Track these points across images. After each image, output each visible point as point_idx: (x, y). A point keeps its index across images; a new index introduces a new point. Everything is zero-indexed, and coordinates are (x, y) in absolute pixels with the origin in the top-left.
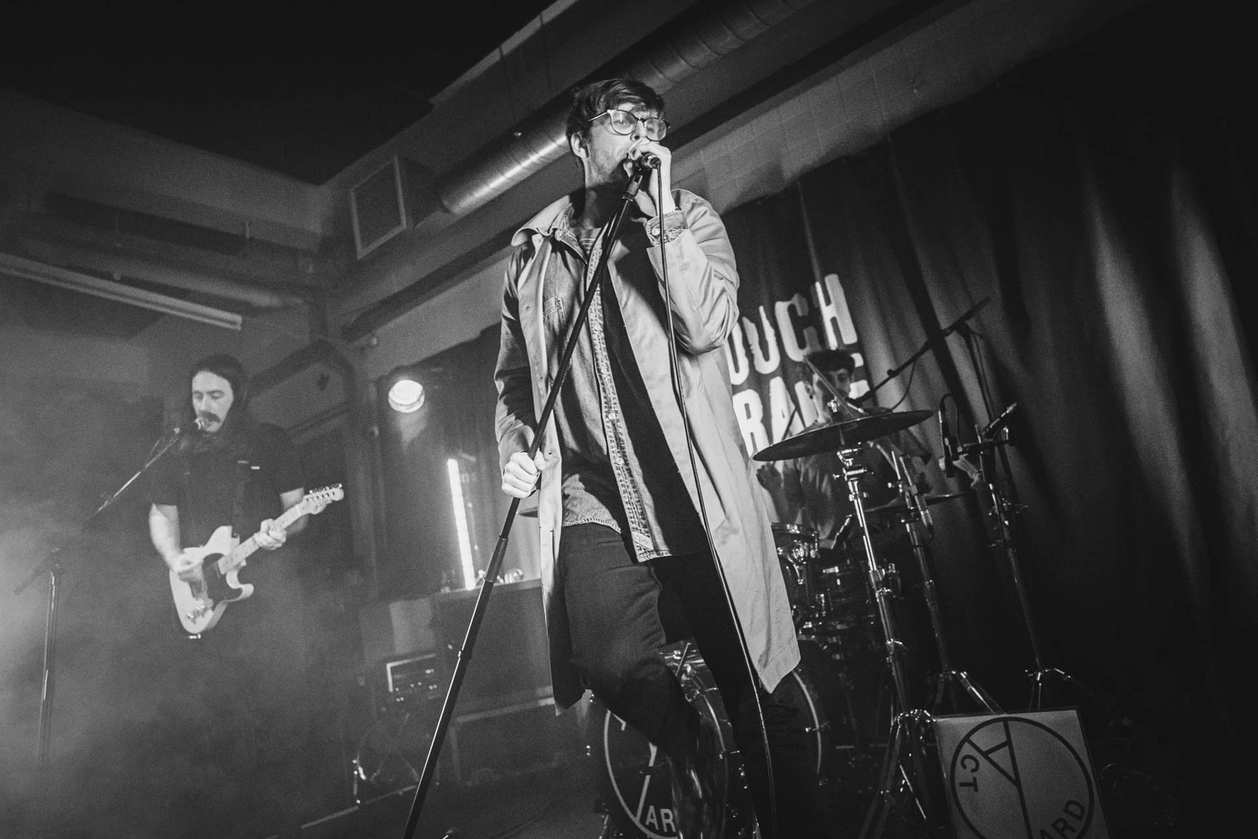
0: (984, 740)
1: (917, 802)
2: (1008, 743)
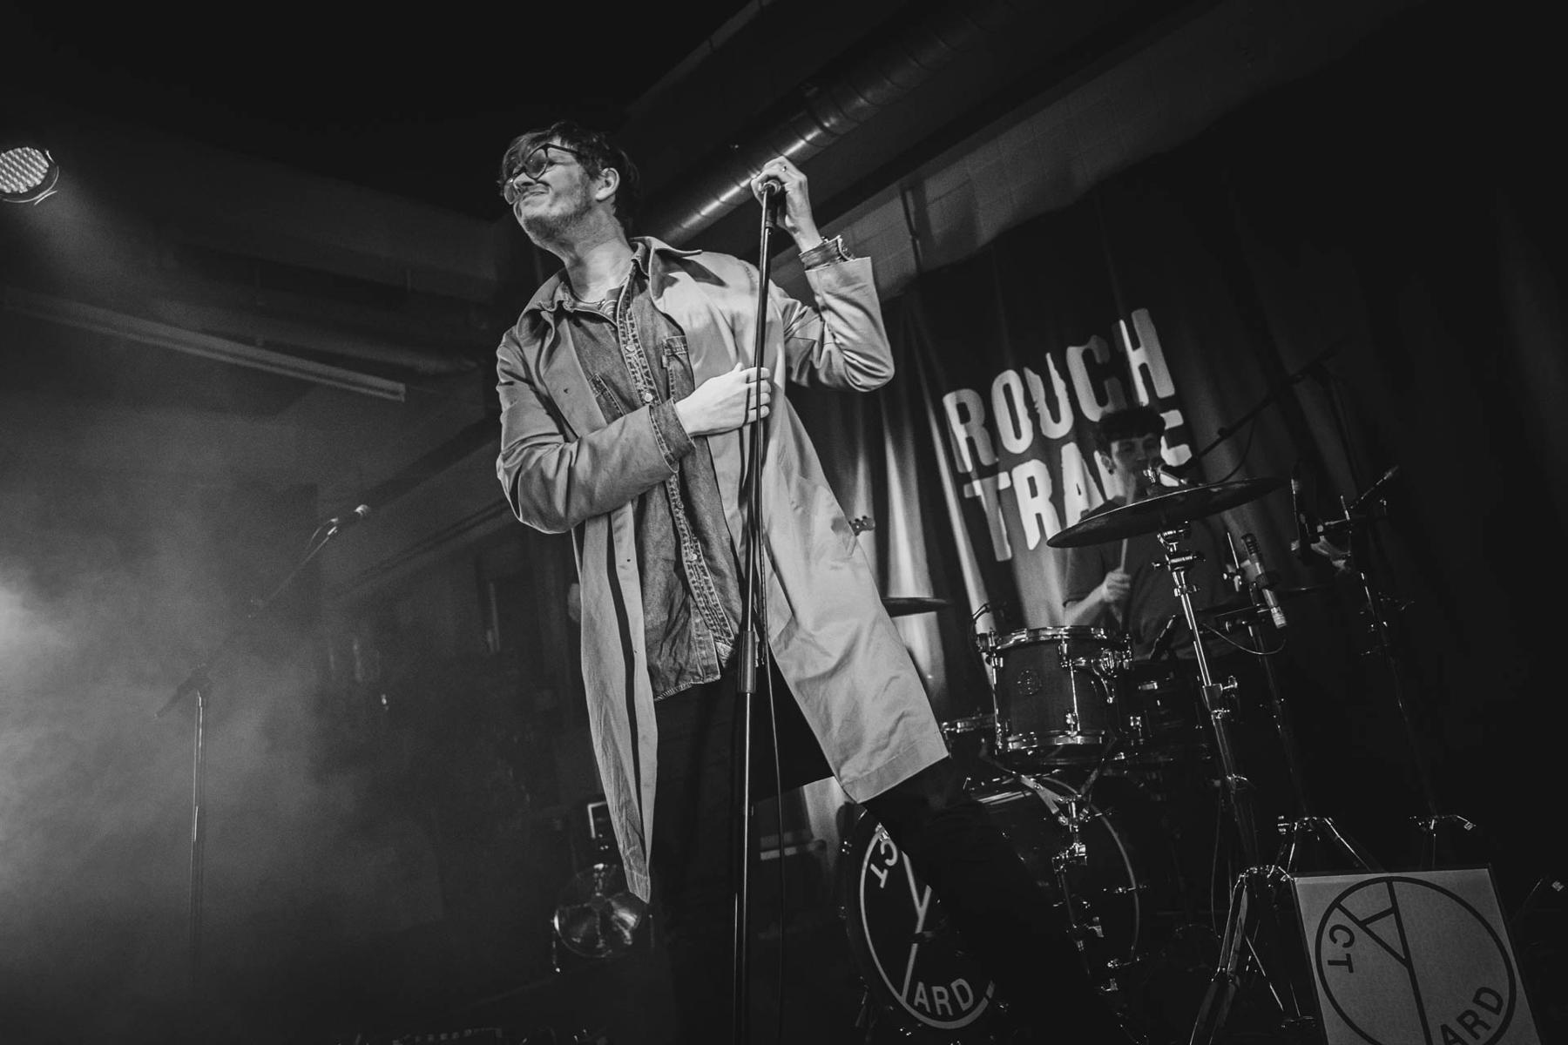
0: (1360, 905)
2: (1394, 910)
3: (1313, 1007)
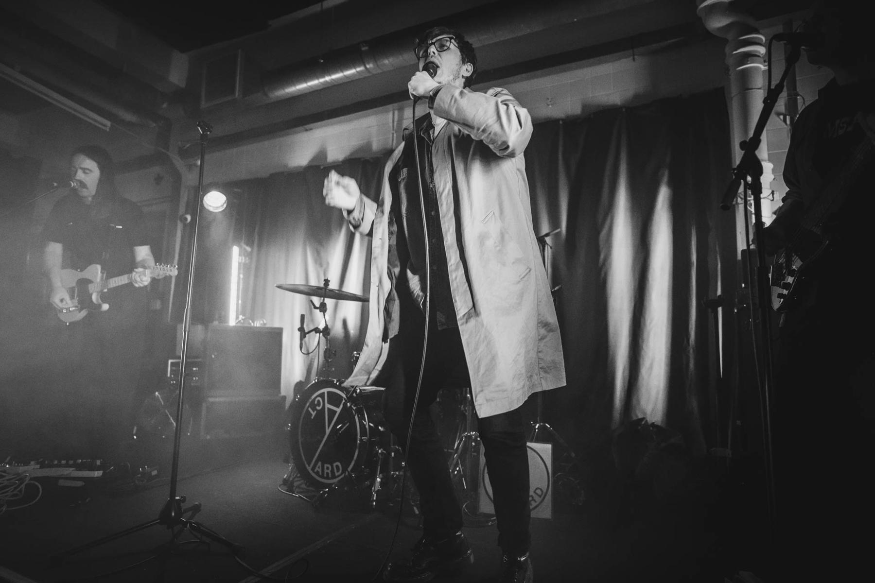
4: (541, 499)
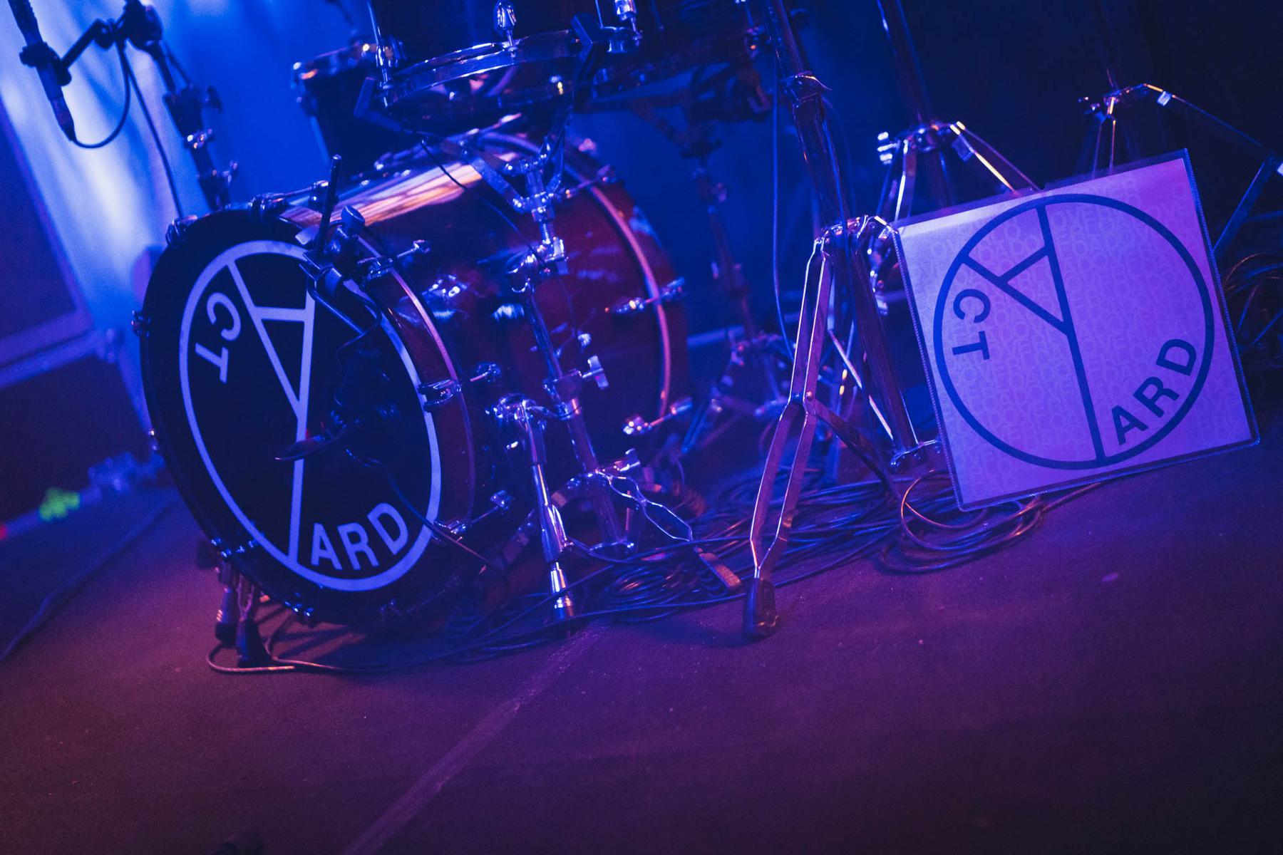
0: (995, 254)
1: (872, 404)
2: (1048, 249)
3: (930, 424)
4: (1192, 380)
